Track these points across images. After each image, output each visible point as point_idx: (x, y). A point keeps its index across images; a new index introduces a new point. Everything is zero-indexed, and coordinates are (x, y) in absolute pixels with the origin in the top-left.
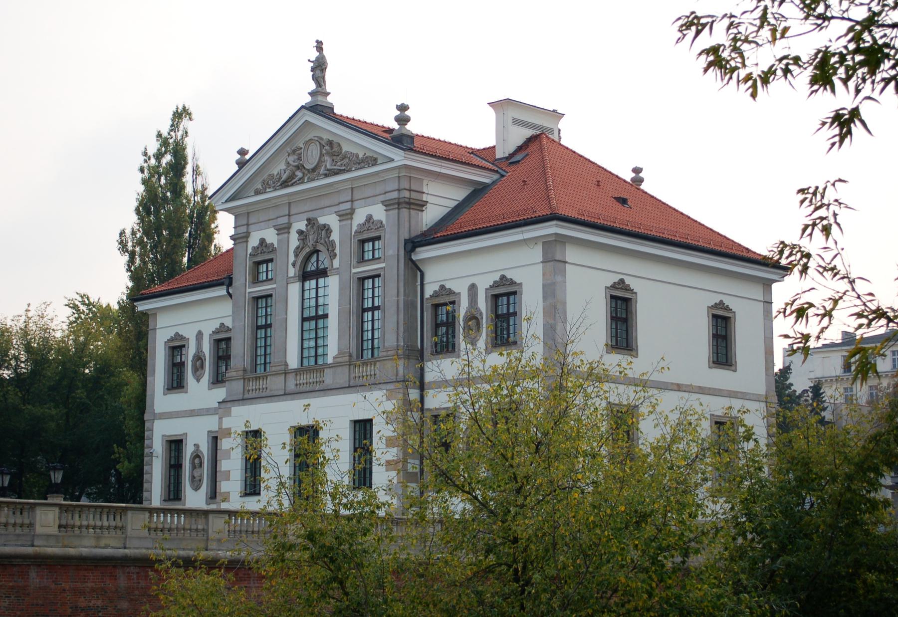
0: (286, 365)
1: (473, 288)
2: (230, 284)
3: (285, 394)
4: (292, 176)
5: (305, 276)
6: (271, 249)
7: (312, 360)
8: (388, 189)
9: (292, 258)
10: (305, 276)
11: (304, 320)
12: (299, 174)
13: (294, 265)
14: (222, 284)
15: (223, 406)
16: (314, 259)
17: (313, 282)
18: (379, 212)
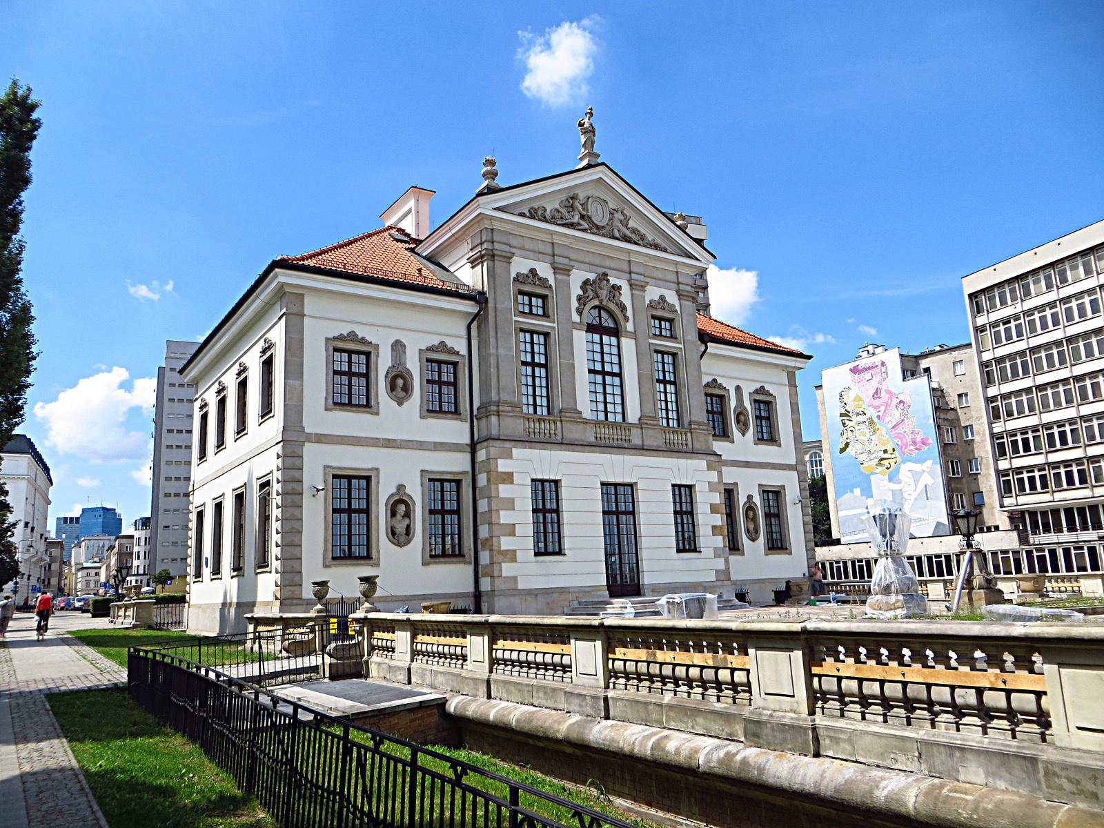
0: (581, 413)
1: (738, 388)
3: (562, 443)
4: (578, 224)
6: (544, 282)
7: (531, 409)
9: (575, 304)
12: (585, 225)
13: (580, 312)
17: (596, 337)
18: (672, 298)
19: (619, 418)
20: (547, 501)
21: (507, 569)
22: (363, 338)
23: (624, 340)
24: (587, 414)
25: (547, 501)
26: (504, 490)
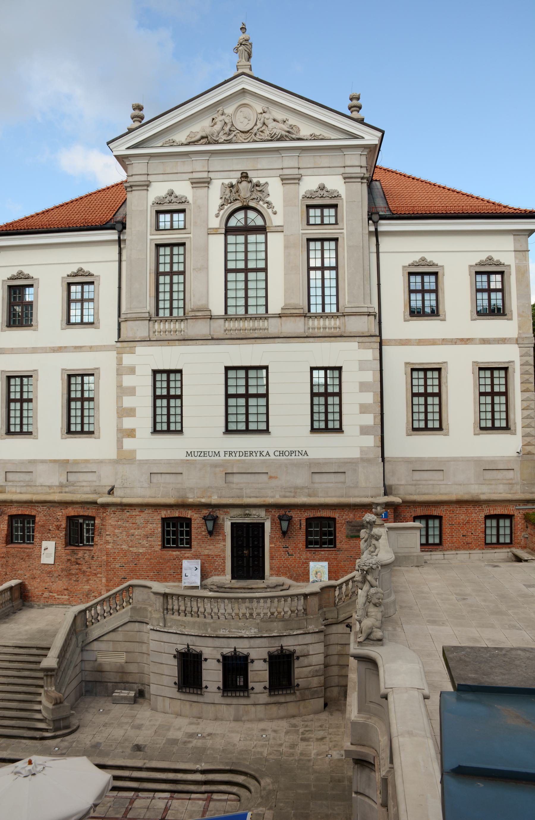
2: (124, 227)
5: (229, 231)
8: (348, 163)
10: (229, 231)
11: (227, 271)
14: (113, 228)
15: (119, 345)
16: (240, 215)
17: (241, 239)
18: (335, 183)
19: (262, 310)
20: (167, 389)
21: (128, 444)
22: (498, 261)
23: (269, 234)
24: (218, 309)
25: (167, 389)
26: (128, 381)
